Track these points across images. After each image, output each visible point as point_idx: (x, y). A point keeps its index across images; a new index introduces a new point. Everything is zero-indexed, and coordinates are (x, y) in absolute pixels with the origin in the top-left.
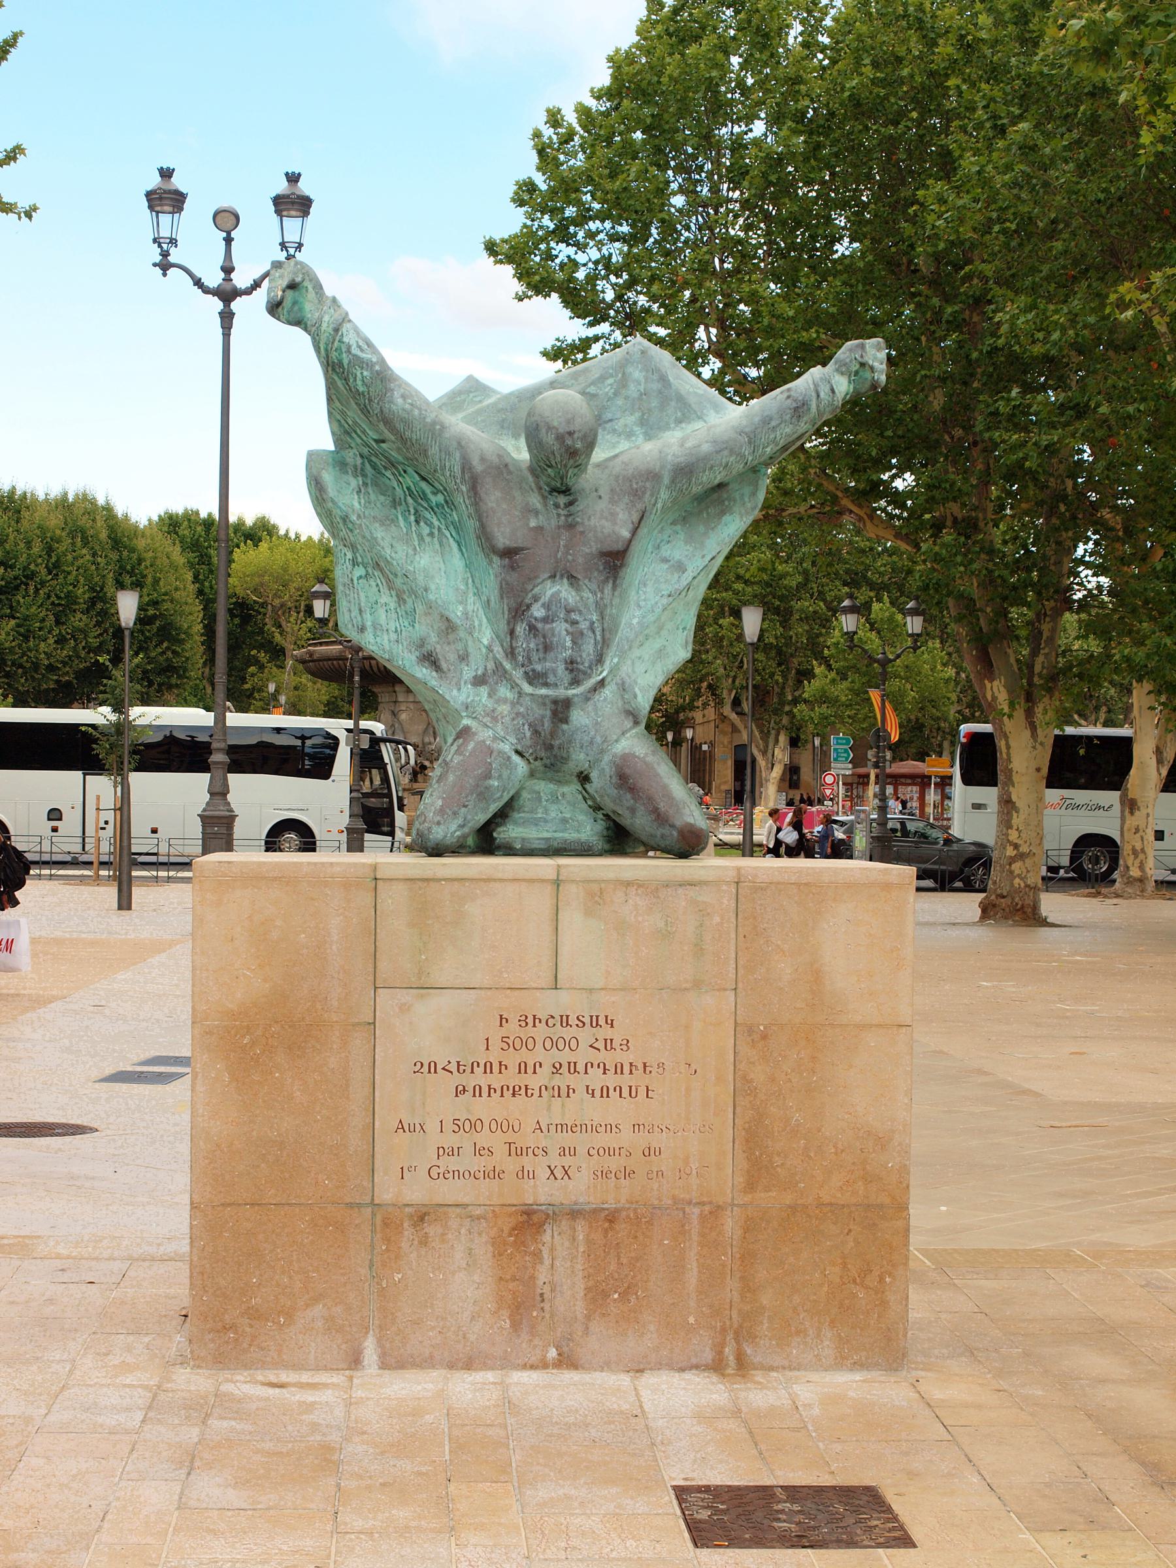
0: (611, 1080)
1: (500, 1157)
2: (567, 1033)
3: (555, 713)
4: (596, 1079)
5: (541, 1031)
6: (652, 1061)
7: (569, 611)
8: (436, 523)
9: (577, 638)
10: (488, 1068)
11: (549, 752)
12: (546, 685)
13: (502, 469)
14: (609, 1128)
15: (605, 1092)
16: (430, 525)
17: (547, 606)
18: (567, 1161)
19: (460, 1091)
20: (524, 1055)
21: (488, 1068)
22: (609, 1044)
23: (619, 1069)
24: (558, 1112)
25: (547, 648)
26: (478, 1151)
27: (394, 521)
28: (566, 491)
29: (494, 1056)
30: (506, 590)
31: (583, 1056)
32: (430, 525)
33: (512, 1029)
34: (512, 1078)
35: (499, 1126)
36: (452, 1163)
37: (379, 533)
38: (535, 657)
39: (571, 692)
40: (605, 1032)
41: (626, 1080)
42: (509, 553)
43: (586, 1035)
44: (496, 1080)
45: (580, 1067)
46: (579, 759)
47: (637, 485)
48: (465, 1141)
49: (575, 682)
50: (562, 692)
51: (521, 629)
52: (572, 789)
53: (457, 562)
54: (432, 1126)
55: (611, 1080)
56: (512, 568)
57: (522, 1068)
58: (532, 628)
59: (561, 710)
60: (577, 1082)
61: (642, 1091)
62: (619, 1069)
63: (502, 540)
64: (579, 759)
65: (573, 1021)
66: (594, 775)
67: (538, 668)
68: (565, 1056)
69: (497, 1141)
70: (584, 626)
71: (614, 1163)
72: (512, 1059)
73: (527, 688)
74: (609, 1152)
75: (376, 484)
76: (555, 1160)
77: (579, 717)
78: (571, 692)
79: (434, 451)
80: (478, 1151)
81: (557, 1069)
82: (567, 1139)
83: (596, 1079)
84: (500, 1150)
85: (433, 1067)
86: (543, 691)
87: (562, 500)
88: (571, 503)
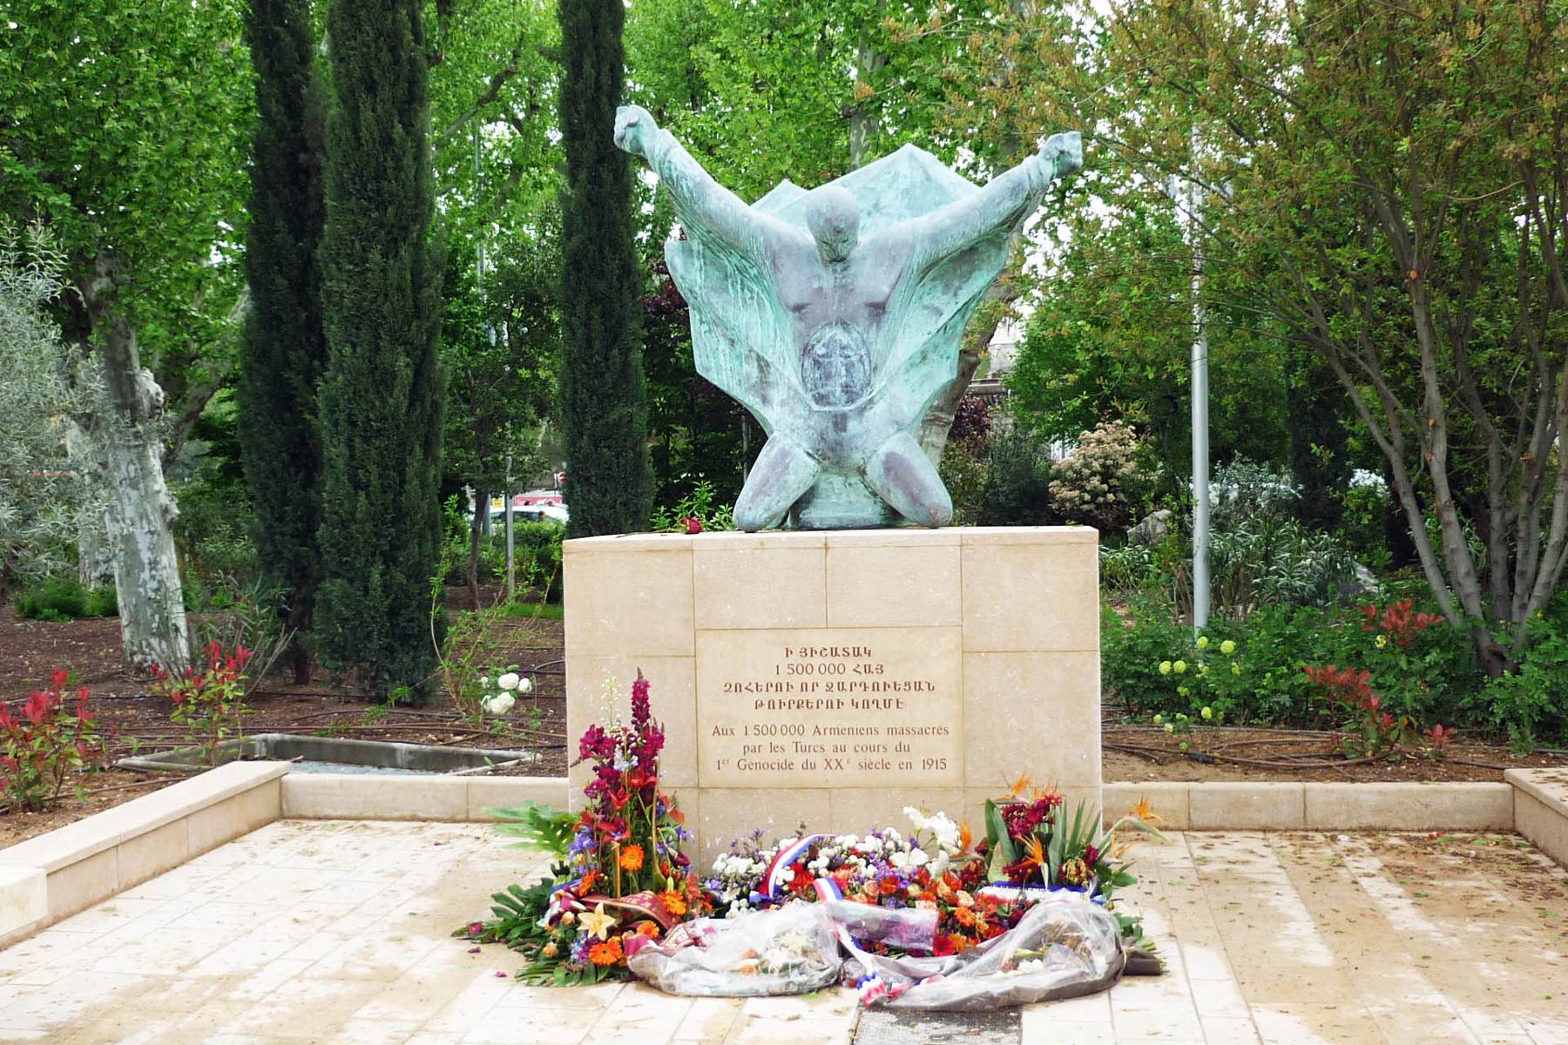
0: (871, 695)
1: (790, 755)
2: (837, 661)
3: (836, 424)
4: (859, 694)
5: (817, 661)
6: (901, 682)
7: (843, 348)
8: (756, 289)
9: (849, 368)
10: (779, 688)
11: (833, 453)
12: (829, 404)
13: (792, 249)
14: (870, 731)
15: (866, 704)
16: (751, 291)
17: (826, 346)
18: (839, 756)
19: (759, 705)
20: (805, 678)
21: (779, 688)
22: (868, 669)
23: (876, 687)
24: (828, 718)
25: (828, 376)
26: (773, 749)
27: (726, 290)
28: (842, 260)
29: (784, 679)
30: (798, 336)
31: (849, 677)
32: (751, 291)
33: (795, 659)
34: (795, 695)
35: (786, 730)
36: (753, 758)
37: (714, 299)
38: (819, 383)
39: (847, 408)
40: (864, 660)
41: (880, 696)
42: (798, 308)
43: (851, 663)
44: (785, 696)
45: (847, 686)
46: (857, 457)
47: (887, 252)
48: (764, 741)
49: (851, 401)
50: (840, 409)
51: (808, 363)
52: (855, 479)
53: (769, 314)
54: (739, 731)
55: (871, 695)
56: (801, 319)
57: (804, 687)
58: (816, 362)
59: (840, 422)
60: (846, 697)
61: (894, 704)
62: (876, 687)
63: (794, 299)
64: (857, 457)
65: (840, 652)
66: (868, 470)
67: (822, 391)
68: (836, 678)
69: (786, 741)
70: (854, 359)
71: (875, 757)
72: (796, 681)
73: (815, 407)
74: (872, 749)
75: (713, 263)
76: (833, 756)
77: (853, 426)
78: (847, 408)
79: (744, 234)
80: (773, 749)
81: (829, 688)
82: (840, 740)
83: (859, 694)
84: (790, 748)
85: (738, 688)
86: (827, 408)
87: (839, 267)
88: (845, 269)
